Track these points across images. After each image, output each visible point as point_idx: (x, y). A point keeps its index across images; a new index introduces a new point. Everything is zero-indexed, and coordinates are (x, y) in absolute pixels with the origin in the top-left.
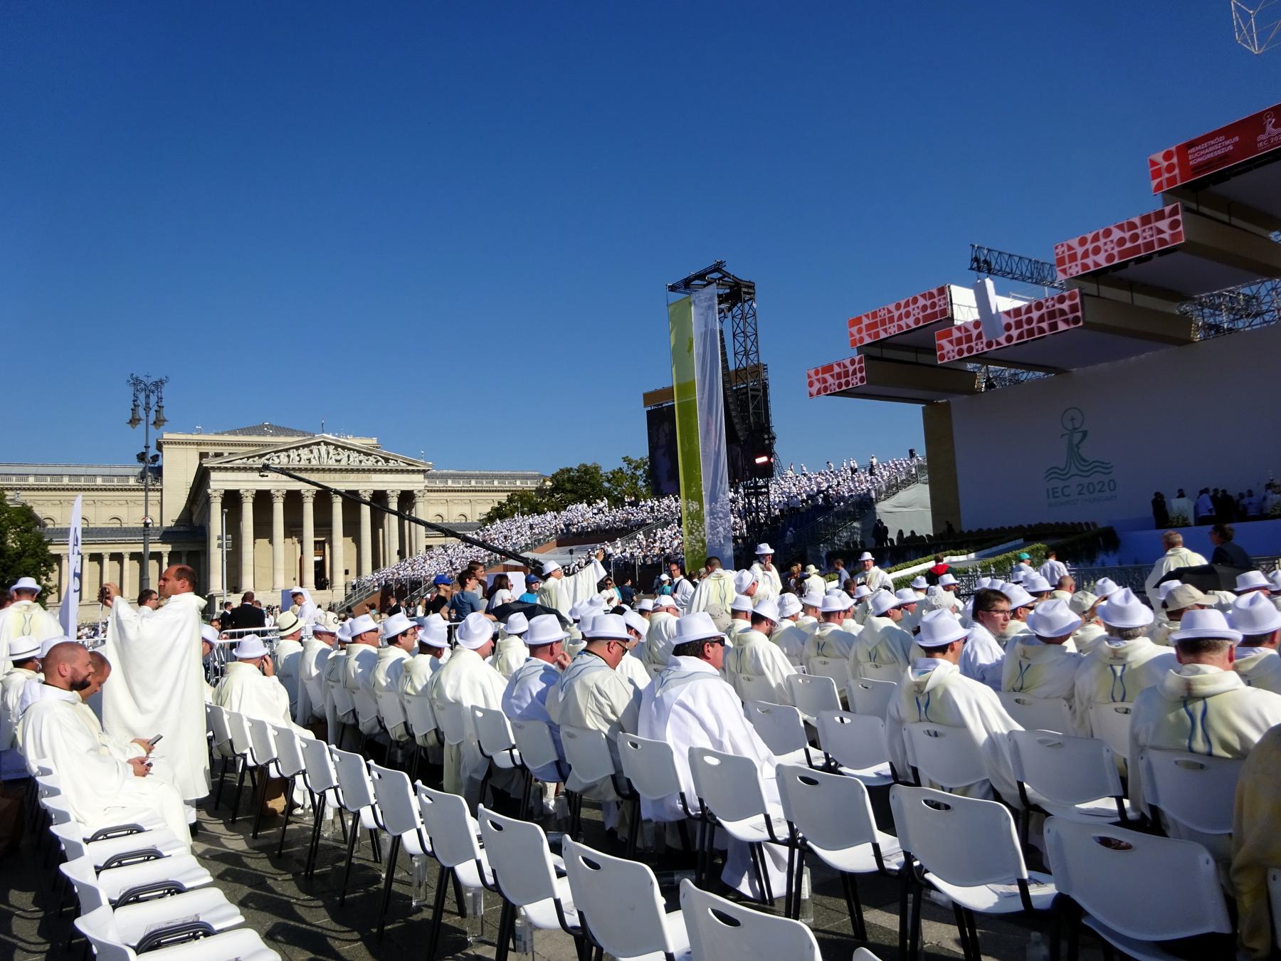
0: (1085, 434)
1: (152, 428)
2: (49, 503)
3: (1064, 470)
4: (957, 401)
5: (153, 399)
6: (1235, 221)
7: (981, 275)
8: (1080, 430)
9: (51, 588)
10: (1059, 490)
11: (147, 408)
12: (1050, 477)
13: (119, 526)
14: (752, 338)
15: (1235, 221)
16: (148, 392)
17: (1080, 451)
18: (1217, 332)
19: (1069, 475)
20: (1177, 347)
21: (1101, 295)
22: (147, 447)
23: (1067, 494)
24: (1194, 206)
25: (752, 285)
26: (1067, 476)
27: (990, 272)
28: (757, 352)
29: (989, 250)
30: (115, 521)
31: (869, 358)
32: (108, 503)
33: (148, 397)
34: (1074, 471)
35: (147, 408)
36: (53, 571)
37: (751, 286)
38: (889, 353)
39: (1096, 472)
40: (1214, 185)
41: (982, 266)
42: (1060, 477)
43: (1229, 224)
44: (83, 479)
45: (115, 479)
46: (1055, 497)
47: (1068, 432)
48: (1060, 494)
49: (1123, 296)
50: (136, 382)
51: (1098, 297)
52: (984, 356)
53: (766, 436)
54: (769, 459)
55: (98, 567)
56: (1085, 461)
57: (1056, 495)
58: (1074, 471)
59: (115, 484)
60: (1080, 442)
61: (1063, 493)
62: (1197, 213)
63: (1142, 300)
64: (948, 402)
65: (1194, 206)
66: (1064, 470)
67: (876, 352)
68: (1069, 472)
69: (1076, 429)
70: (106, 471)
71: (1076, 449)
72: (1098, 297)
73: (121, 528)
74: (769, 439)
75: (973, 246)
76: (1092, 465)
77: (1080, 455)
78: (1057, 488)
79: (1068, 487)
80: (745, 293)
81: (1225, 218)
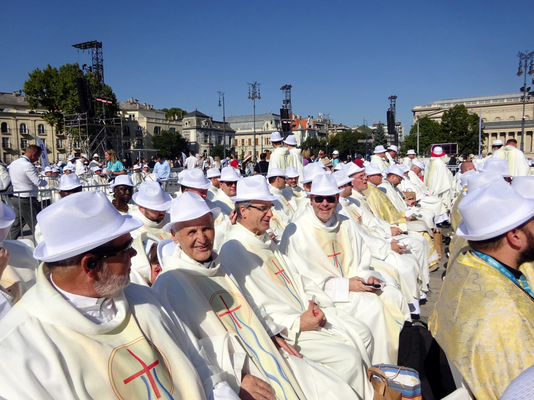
1: (528, 75)
2: (485, 112)
5: (529, 61)
9: (484, 147)
11: (526, 66)
13: (499, 121)
16: (526, 58)
22: (525, 84)
30: (512, 118)
32: (509, 110)
33: (526, 61)
35: (526, 66)
36: (485, 140)
44: (498, 101)
45: (513, 100)
50: (521, 55)
55: (504, 138)
59: (513, 102)
70: (509, 96)
73: (514, 121)
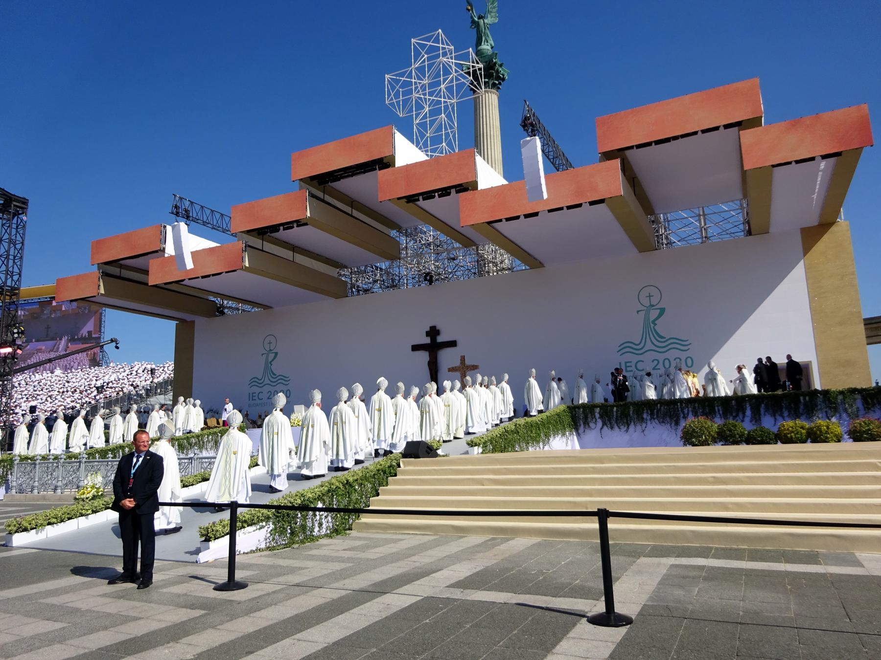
0: (276, 354)
3: (261, 380)
4: (200, 322)
6: (356, 213)
7: (178, 218)
8: (273, 351)
10: (257, 395)
12: (251, 385)
14: (18, 246)
15: (356, 213)
17: (272, 368)
18: (358, 291)
19: (264, 383)
20: (334, 299)
21: (264, 249)
23: (261, 398)
24: (320, 194)
25: (26, 201)
26: (262, 385)
27: (187, 217)
28: (21, 258)
29: (192, 203)
31: (105, 275)
34: (267, 381)
37: (25, 202)
38: (126, 273)
39: (280, 383)
40: (331, 183)
41: (181, 213)
42: (258, 385)
43: (351, 216)
46: (253, 400)
47: (266, 352)
48: (256, 398)
49: (287, 254)
51: (262, 250)
52: (182, 283)
53: (16, 331)
54: (15, 351)
56: (275, 375)
57: (254, 398)
58: (267, 381)
60: (273, 360)
61: (258, 398)
62: (323, 201)
63: (300, 259)
64: (193, 322)
65: (320, 194)
66: (260, 382)
67: (115, 270)
68: (264, 381)
69: (271, 350)
71: (270, 365)
72: (262, 250)
74: (18, 333)
75: (175, 196)
76: (278, 378)
77: (272, 372)
78: (255, 393)
79: (262, 392)
80: (15, 206)
81: (348, 209)
